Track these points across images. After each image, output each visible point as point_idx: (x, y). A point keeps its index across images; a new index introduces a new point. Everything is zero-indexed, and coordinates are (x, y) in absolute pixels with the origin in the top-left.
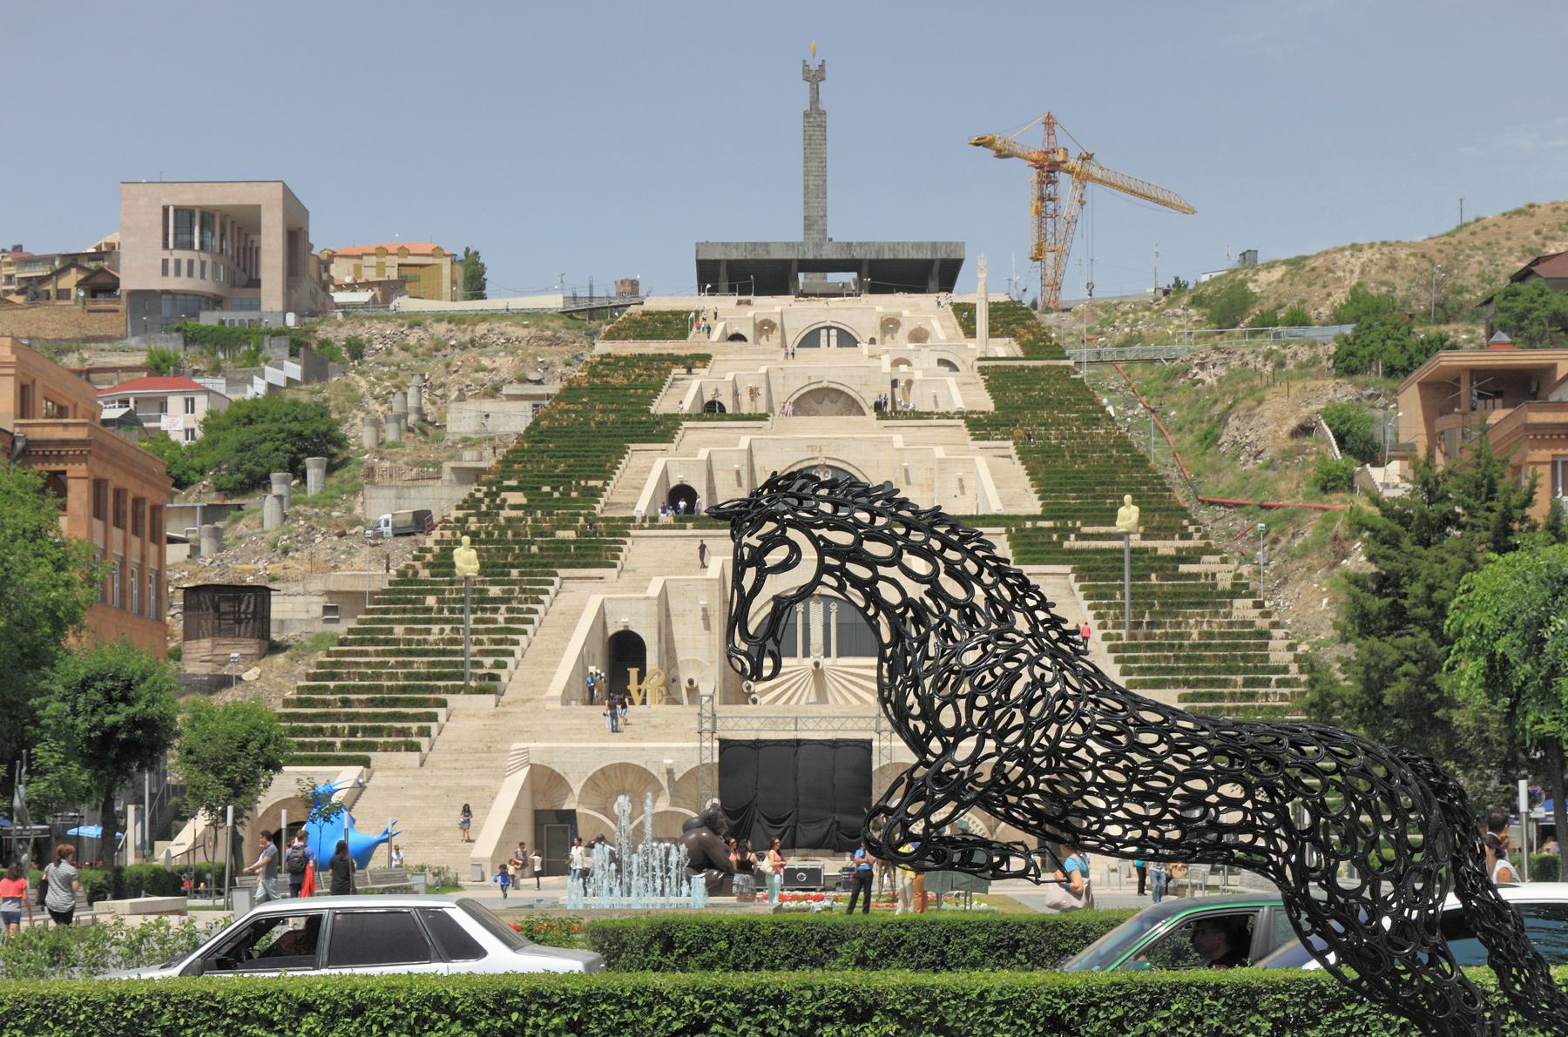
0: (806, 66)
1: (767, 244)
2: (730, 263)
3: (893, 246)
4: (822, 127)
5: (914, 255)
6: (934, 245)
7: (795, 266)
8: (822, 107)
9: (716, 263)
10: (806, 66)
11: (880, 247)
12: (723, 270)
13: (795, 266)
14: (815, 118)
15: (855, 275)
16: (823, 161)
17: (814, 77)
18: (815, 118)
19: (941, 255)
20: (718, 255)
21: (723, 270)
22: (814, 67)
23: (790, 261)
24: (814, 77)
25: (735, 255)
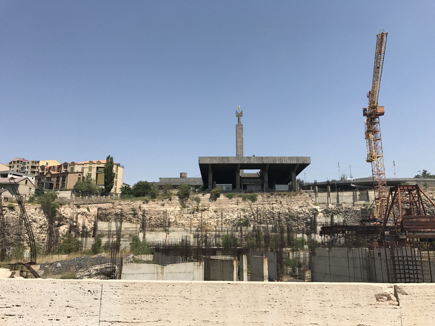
0: (237, 112)
1: (228, 158)
2: (213, 165)
3: (280, 158)
4: (242, 129)
5: (289, 162)
6: (297, 158)
7: (239, 167)
8: (242, 124)
9: (207, 165)
10: (237, 112)
11: (275, 158)
12: (210, 168)
13: (239, 167)
14: (239, 128)
15: (259, 170)
16: (242, 138)
17: (239, 115)
18: (239, 128)
19: (301, 162)
20: (208, 162)
21: (210, 168)
22: (239, 112)
23: (237, 164)
24: (239, 115)
25: (215, 162)
